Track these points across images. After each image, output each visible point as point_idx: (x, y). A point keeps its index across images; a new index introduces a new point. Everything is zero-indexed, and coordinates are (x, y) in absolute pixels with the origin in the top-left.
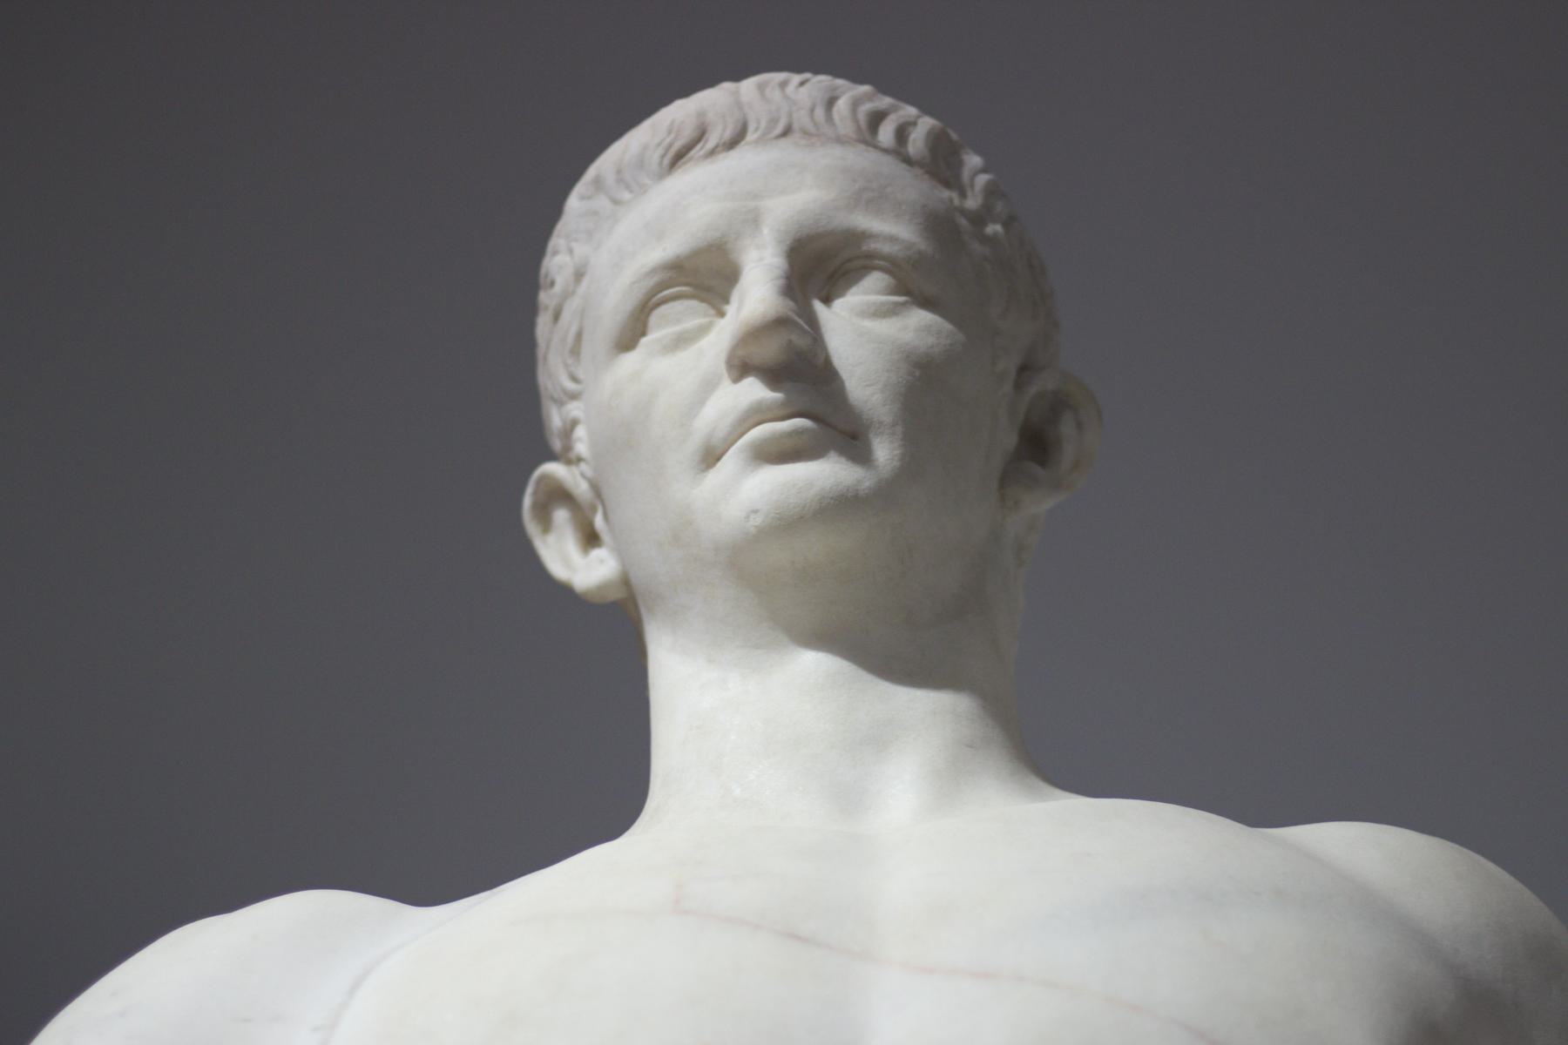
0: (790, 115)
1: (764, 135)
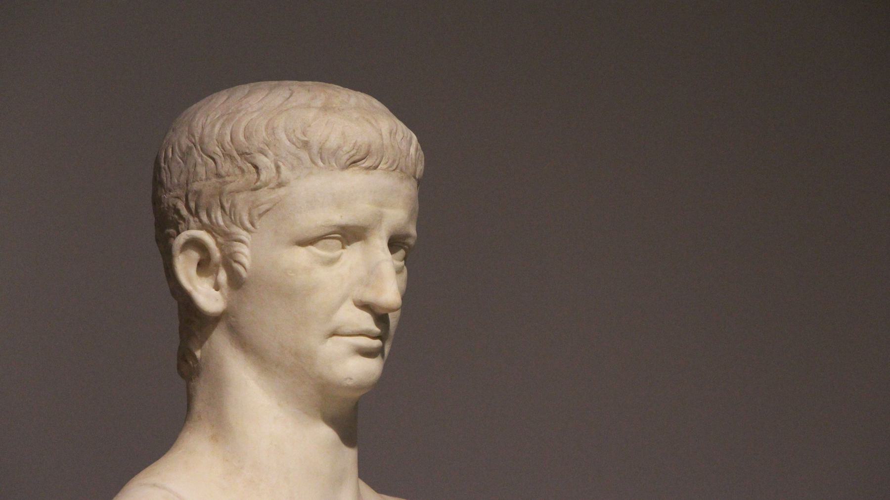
1: (388, 168)
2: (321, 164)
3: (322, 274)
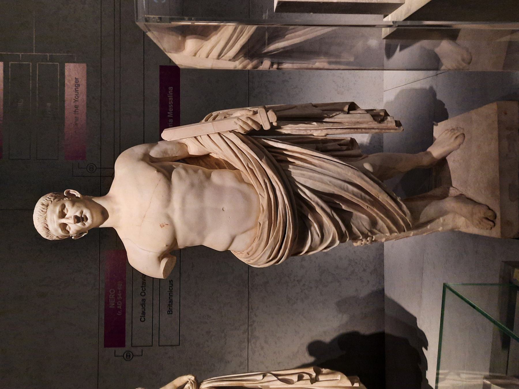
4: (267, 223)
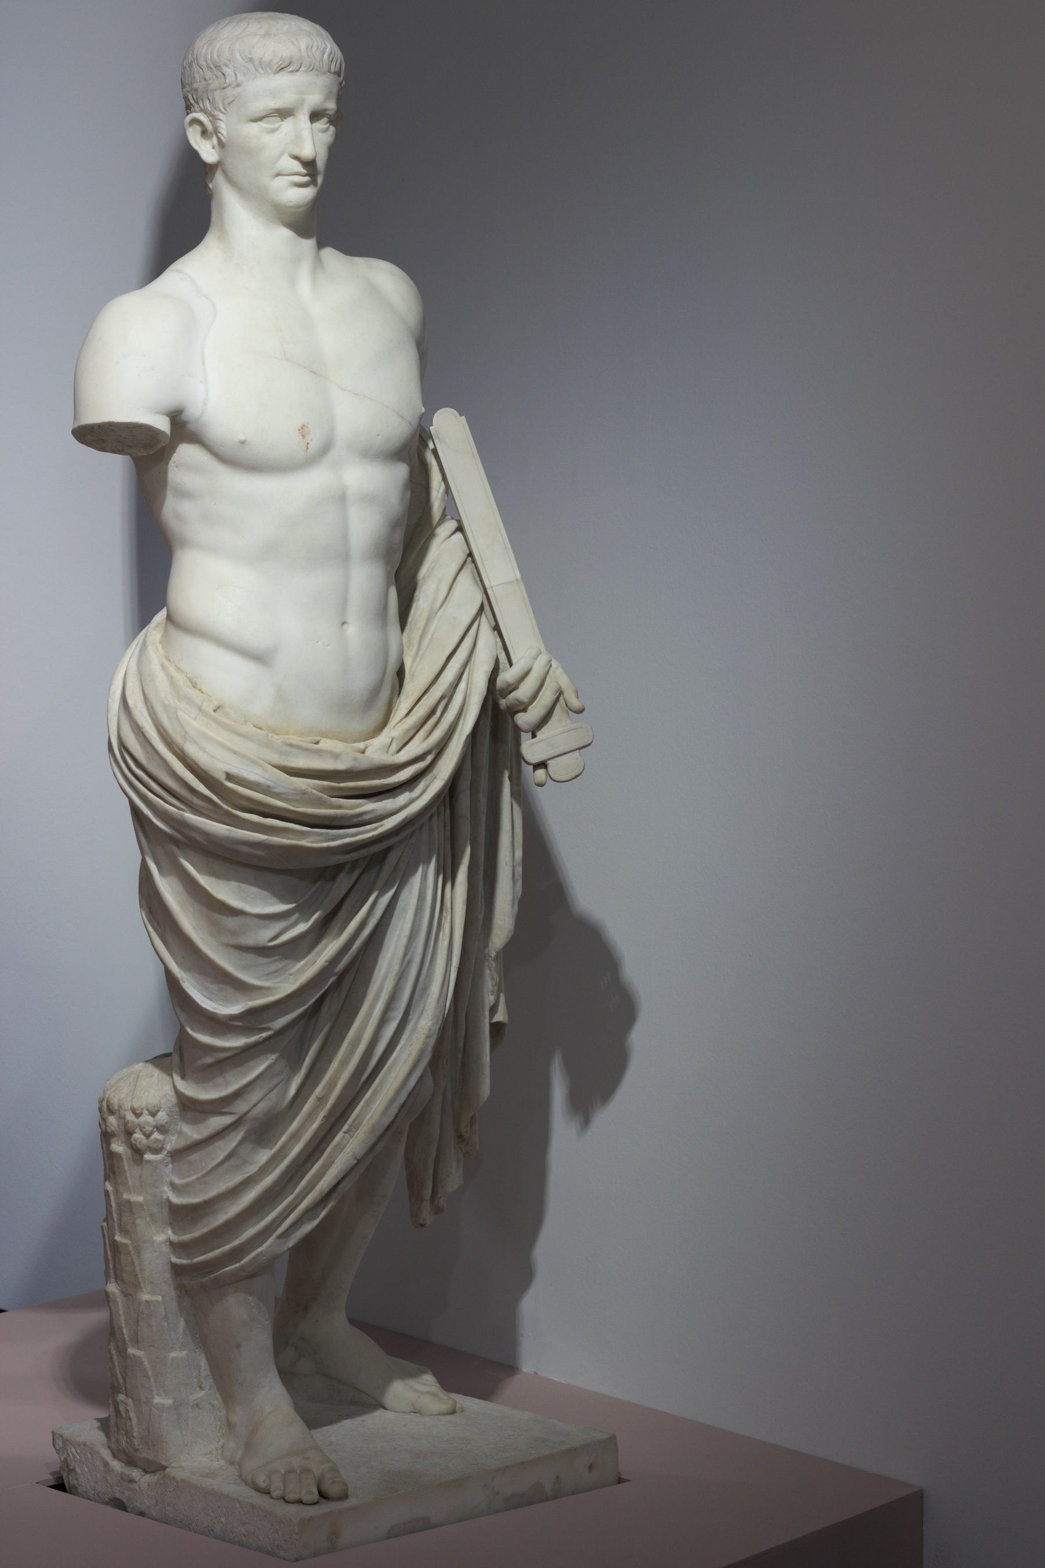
0: (314, 63)
2: (261, 71)
3: (267, 139)
4: (341, 766)
